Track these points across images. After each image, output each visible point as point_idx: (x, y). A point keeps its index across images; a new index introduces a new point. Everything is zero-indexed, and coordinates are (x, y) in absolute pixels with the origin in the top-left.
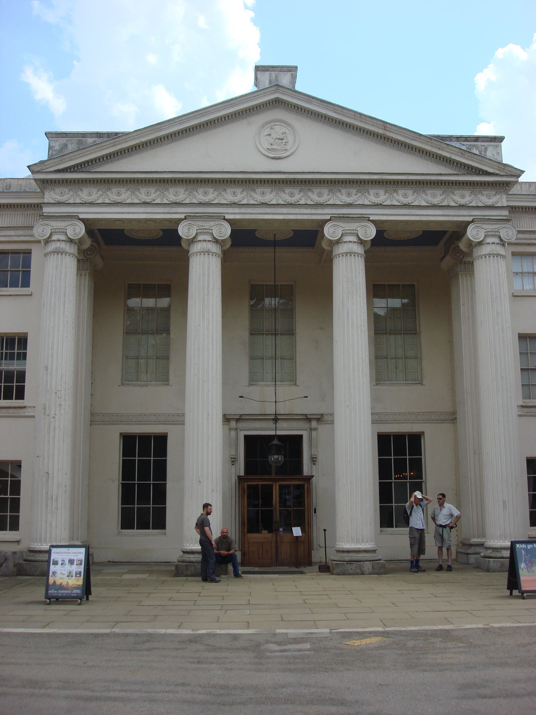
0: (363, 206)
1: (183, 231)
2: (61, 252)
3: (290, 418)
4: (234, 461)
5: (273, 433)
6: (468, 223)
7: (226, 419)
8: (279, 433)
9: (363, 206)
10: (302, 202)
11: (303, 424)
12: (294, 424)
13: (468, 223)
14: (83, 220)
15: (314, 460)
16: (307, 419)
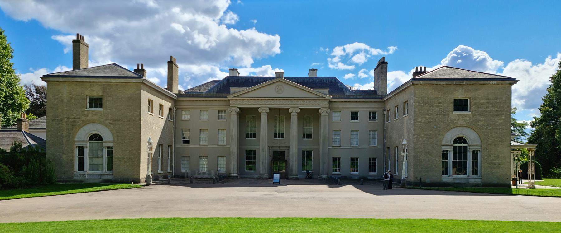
0: (297, 105)
2: (234, 114)
3: (283, 147)
4: (270, 156)
5: (278, 150)
6: (319, 109)
7: (269, 147)
8: (280, 150)
9: (297, 105)
10: (284, 104)
11: (286, 148)
12: (284, 148)
13: (319, 109)
14: (239, 108)
15: (288, 156)
16: (286, 147)
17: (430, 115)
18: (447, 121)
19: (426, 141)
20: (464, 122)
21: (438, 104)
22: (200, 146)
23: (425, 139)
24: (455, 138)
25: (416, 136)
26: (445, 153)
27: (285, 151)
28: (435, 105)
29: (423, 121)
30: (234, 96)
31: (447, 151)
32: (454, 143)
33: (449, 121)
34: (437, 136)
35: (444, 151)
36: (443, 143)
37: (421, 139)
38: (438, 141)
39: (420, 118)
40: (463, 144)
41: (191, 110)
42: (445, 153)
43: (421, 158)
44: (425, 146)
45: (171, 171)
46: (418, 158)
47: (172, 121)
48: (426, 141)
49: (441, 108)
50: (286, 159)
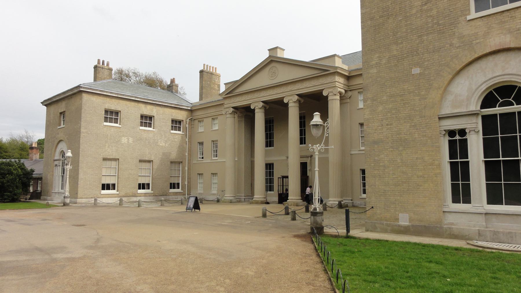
1: (252, 107)
13: (323, 89)
17: (402, 43)
18: (451, 45)
19: (394, 112)
20: (508, 36)
21: (422, 5)
22: (211, 161)
23: (391, 106)
24: (484, 87)
25: (369, 102)
26: (457, 137)
27: (307, 162)
28: (414, 11)
29: (384, 61)
30: (227, 93)
31: (463, 132)
32: (483, 106)
33: (457, 45)
34: (423, 93)
35: (451, 133)
36: (447, 110)
37: (380, 108)
38: (425, 107)
39: (377, 55)
40: (515, 106)
41: (205, 119)
42: (457, 137)
43: (383, 156)
44: (391, 125)
45: (182, 191)
46: (376, 158)
47: (183, 133)
48: (394, 112)
49: (431, 16)
50: (308, 175)
